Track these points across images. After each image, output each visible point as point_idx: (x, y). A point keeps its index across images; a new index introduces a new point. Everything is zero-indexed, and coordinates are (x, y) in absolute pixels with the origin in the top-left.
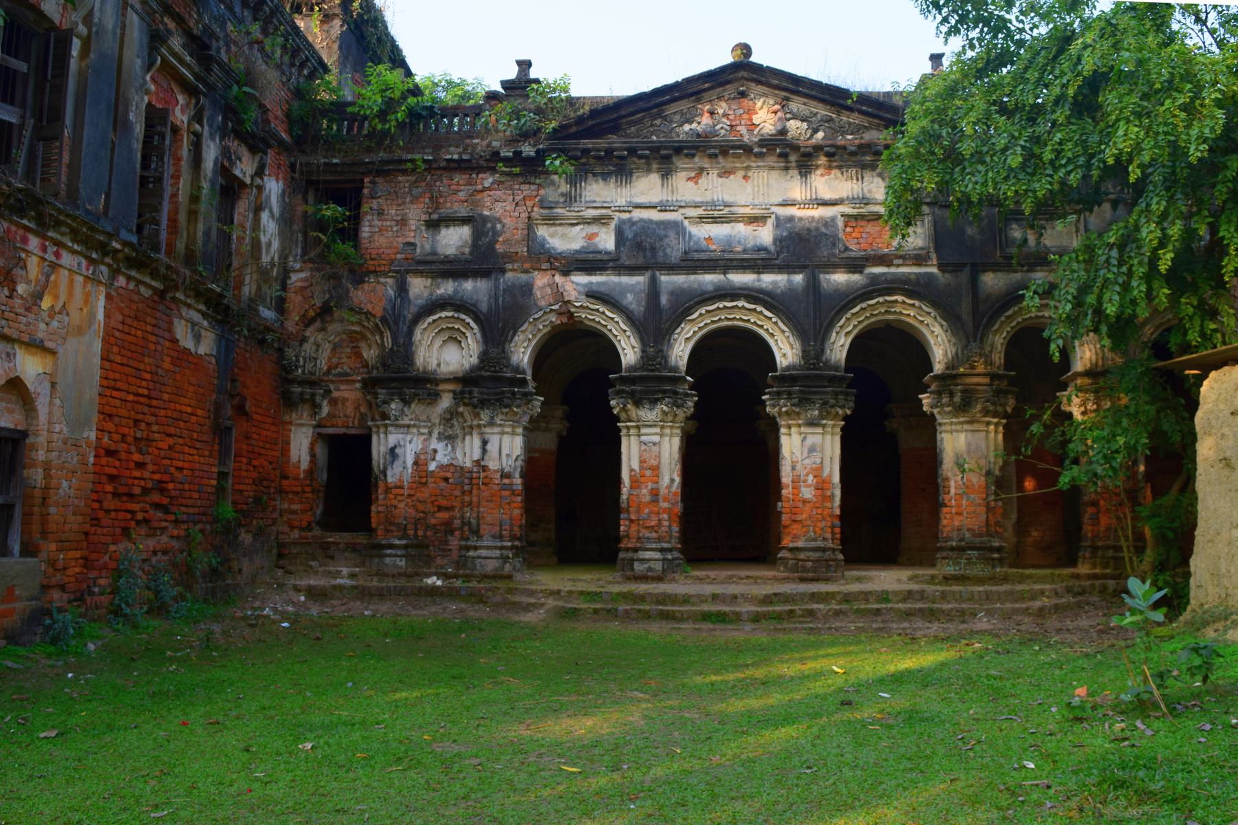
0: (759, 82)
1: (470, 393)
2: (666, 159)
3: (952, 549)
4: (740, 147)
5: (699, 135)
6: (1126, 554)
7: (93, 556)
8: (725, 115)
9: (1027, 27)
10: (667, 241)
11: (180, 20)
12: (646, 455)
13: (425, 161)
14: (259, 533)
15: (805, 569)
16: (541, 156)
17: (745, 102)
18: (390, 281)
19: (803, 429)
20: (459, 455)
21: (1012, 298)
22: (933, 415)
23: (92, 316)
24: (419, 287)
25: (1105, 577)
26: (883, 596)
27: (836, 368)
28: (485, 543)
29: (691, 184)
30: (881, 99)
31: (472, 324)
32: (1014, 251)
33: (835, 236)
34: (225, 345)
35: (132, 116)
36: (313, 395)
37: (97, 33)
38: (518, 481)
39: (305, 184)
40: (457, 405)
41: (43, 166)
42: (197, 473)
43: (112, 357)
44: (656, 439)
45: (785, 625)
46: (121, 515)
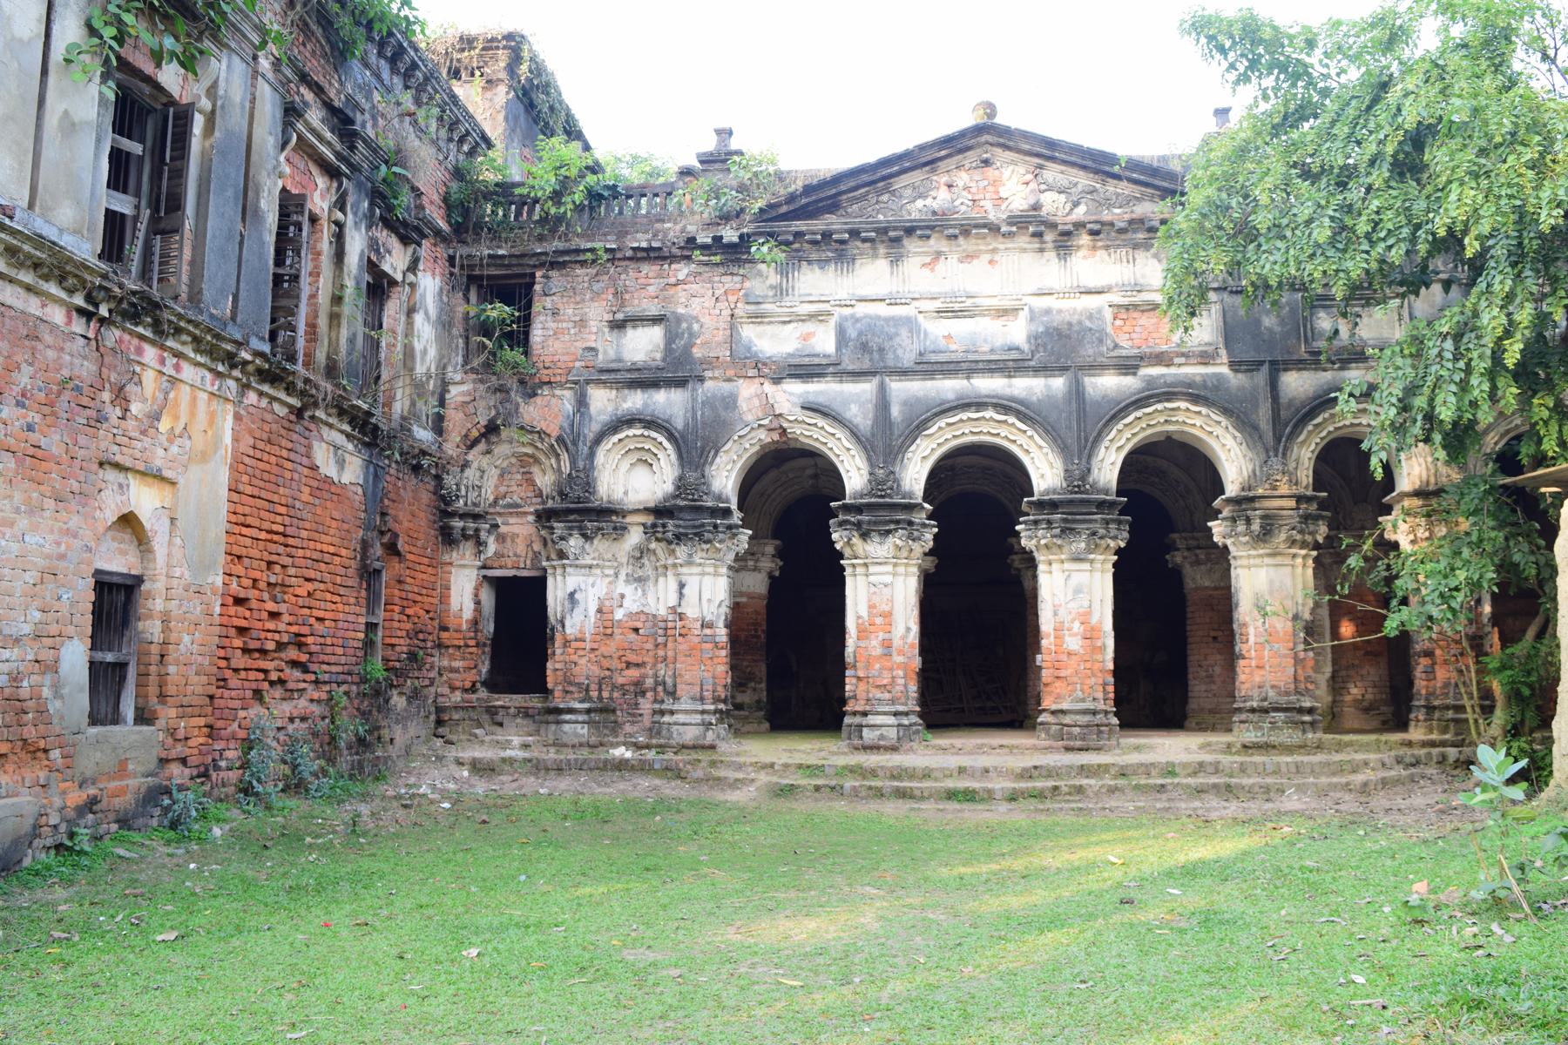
0: (1007, 148)
1: (664, 526)
2: (896, 241)
3: (1253, 710)
4: (984, 226)
5: (934, 213)
6: (1470, 716)
7: (220, 724)
8: (966, 188)
9: (1333, 72)
10: (897, 340)
11: (318, 90)
12: (876, 600)
13: (607, 250)
14: (415, 695)
15: (1071, 737)
16: (745, 240)
17: (990, 171)
18: (568, 394)
19: (1067, 566)
20: (651, 600)
21: (1323, 401)
22: (1226, 547)
23: (218, 440)
24: (603, 402)
25: (1443, 744)
26: (1170, 770)
28: (683, 707)
29: (926, 271)
30: (1155, 164)
31: (666, 443)
32: (1321, 344)
33: (1102, 331)
34: (375, 473)
35: (263, 204)
36: (477, 530)
37: (223, 107)
38: (722, 633)
40: (648, 540)
41: (161, 264)
42: (341, 624)
43: (241, 487)
45: (1048, 804)
46: (253, 675)
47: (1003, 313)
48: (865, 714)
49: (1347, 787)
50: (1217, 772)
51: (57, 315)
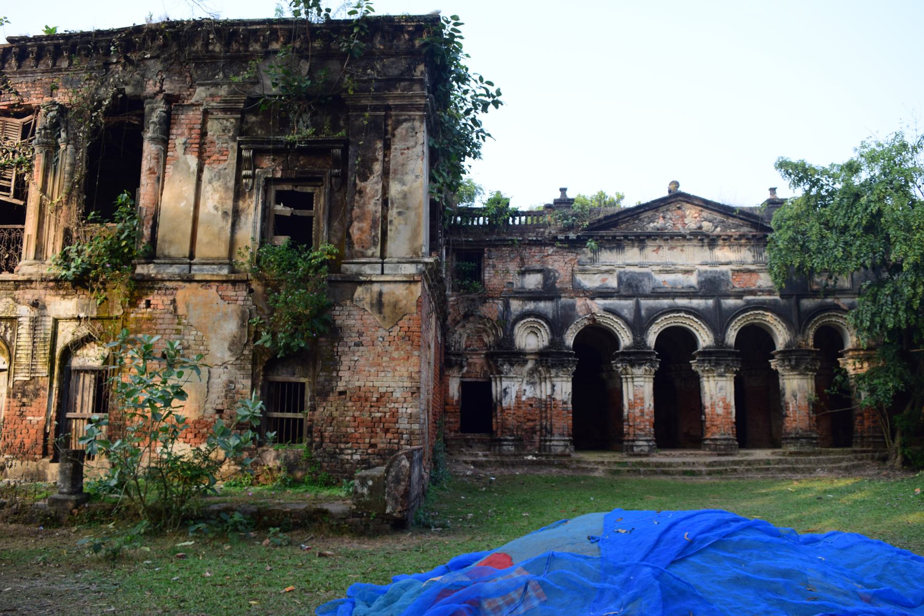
1: (547, 360)
3: (792, 438)
5: (658, 229)
8: (671, 219)
10: (643, 283)
12: (637, 392)
15: (720, 450)
18: (500, 302)
22: (776, 370)
24: (516, 306)
25: (868, 451)
26: (758, 462)
27: (730, 347)
29: (654, 253)
33: (728, 281)
38: (570, 406)
44: (642, 384)
47: (687, 272)
48: (634, 441)
49: (839, 468)
50: (786, 463)
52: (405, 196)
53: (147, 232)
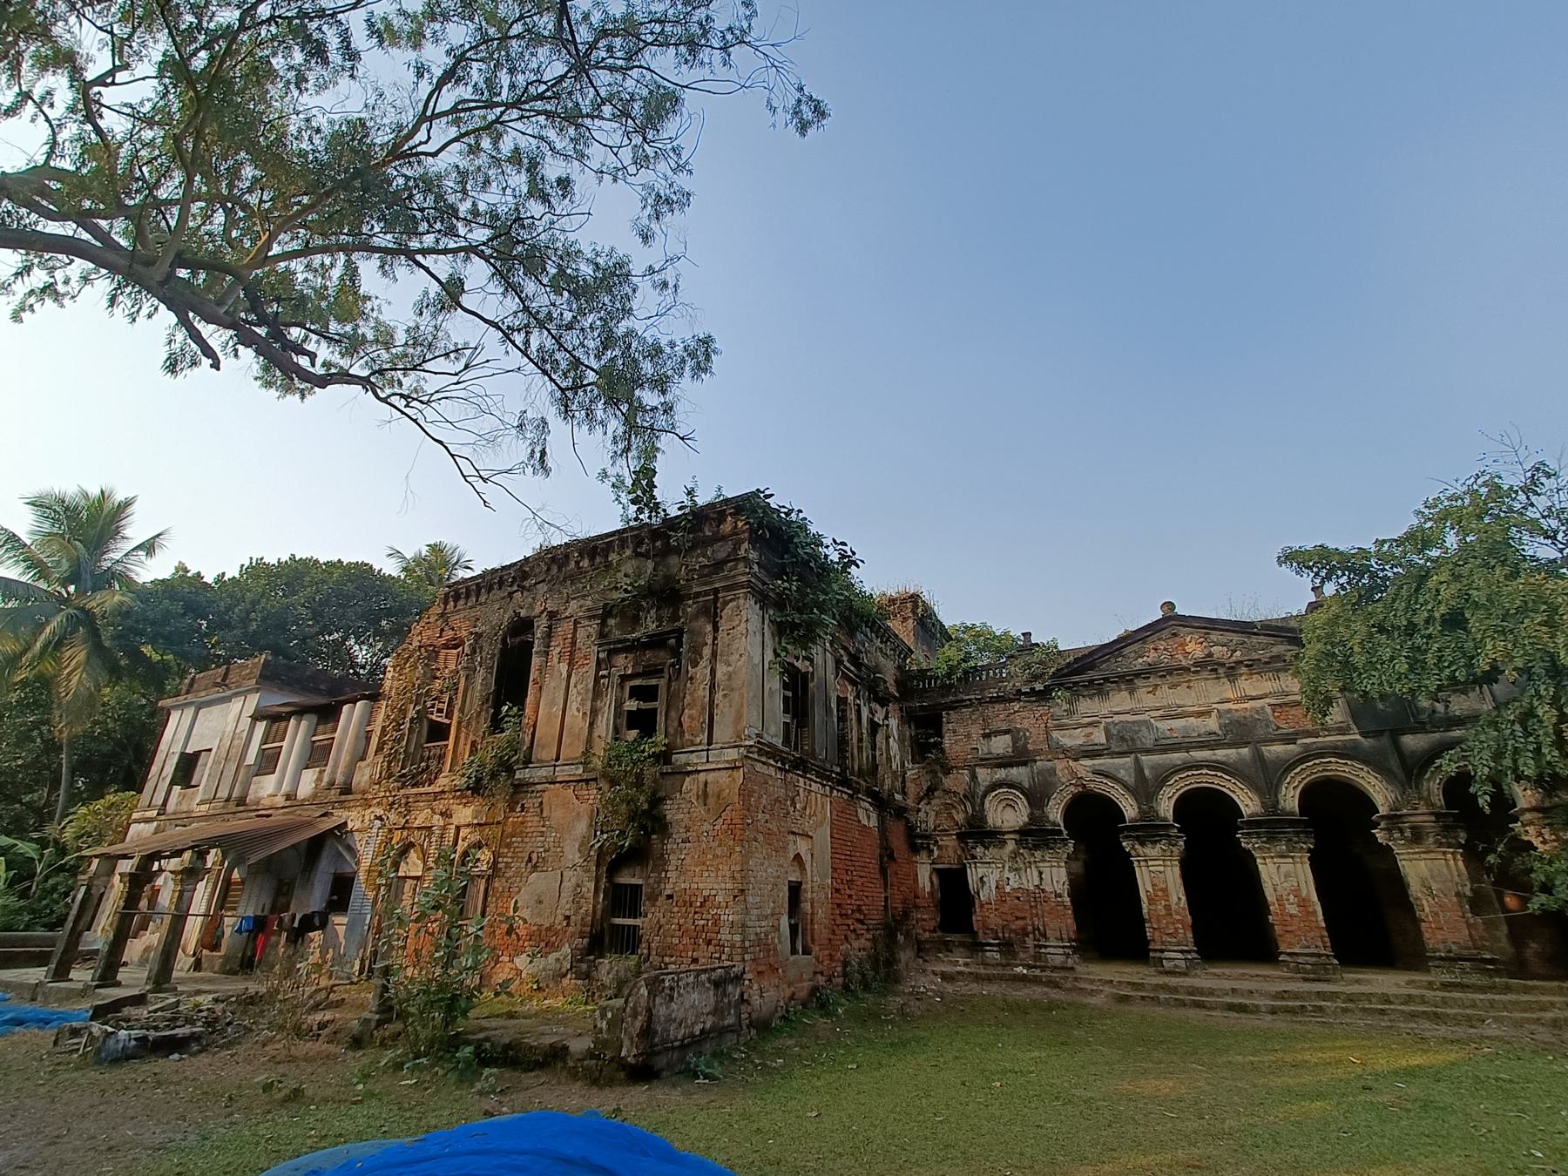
32: (1424, 717)
39: (908, 718)
51: (772, 771)
52: (730, 677)
53: (528, 739)
